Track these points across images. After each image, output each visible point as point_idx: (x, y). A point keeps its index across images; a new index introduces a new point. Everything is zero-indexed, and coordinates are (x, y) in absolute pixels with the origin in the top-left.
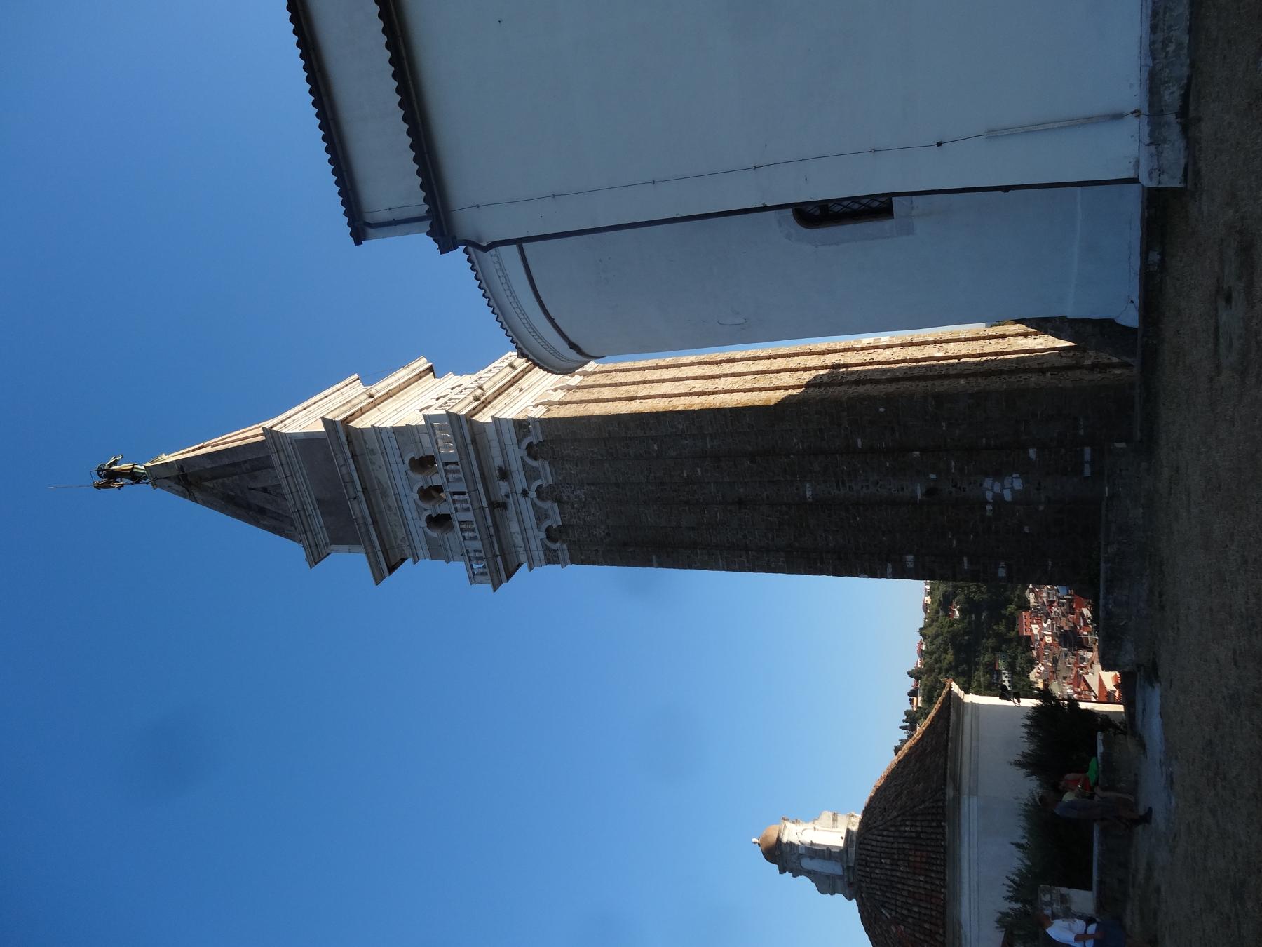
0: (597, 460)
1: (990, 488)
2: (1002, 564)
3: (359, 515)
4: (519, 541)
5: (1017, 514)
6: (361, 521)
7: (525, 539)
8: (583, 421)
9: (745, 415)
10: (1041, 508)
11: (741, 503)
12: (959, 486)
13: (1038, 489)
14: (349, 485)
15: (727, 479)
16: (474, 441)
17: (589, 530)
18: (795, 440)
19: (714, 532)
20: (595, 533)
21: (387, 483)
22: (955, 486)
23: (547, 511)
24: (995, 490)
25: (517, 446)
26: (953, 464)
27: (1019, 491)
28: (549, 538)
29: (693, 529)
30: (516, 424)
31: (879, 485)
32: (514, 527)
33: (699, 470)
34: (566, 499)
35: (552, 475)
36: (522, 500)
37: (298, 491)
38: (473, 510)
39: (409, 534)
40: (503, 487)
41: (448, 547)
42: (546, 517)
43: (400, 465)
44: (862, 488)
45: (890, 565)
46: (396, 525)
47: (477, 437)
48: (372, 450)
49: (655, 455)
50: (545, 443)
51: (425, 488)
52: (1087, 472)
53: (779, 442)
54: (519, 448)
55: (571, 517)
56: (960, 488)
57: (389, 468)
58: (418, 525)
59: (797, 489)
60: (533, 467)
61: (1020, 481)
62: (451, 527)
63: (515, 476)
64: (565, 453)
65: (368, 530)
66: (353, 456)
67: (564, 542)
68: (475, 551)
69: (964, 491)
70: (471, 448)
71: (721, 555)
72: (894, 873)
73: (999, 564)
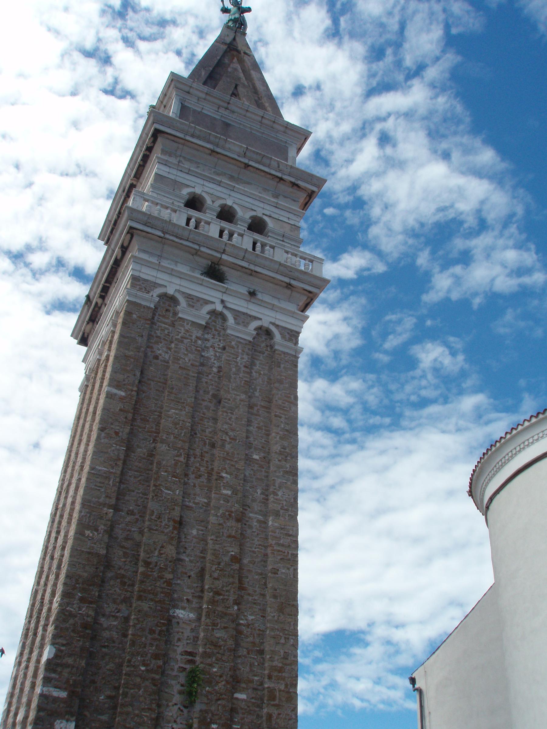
3: (227, 146)
7: (171, 273)
8: (292, 397)
9: (288, 569)
16: (289, 286)
17: (164, 339)
18: (251, 618)
20: (161, 345)
21: (244, 187)
28: (164, 296)
30: (297, 335)
33: (229, 492)
34: (206, 336)
35: (238, 337)
45: (63, 694)
47: (288, 292)
50: (269, 349)
54: (271, 323)
55: (187, 331)
57: (261, 200)
59: (188, 600)
60: (248, 324)
63: (243, 303)
64: (258, 363)
65: (209, 142)
66: (281, 179)
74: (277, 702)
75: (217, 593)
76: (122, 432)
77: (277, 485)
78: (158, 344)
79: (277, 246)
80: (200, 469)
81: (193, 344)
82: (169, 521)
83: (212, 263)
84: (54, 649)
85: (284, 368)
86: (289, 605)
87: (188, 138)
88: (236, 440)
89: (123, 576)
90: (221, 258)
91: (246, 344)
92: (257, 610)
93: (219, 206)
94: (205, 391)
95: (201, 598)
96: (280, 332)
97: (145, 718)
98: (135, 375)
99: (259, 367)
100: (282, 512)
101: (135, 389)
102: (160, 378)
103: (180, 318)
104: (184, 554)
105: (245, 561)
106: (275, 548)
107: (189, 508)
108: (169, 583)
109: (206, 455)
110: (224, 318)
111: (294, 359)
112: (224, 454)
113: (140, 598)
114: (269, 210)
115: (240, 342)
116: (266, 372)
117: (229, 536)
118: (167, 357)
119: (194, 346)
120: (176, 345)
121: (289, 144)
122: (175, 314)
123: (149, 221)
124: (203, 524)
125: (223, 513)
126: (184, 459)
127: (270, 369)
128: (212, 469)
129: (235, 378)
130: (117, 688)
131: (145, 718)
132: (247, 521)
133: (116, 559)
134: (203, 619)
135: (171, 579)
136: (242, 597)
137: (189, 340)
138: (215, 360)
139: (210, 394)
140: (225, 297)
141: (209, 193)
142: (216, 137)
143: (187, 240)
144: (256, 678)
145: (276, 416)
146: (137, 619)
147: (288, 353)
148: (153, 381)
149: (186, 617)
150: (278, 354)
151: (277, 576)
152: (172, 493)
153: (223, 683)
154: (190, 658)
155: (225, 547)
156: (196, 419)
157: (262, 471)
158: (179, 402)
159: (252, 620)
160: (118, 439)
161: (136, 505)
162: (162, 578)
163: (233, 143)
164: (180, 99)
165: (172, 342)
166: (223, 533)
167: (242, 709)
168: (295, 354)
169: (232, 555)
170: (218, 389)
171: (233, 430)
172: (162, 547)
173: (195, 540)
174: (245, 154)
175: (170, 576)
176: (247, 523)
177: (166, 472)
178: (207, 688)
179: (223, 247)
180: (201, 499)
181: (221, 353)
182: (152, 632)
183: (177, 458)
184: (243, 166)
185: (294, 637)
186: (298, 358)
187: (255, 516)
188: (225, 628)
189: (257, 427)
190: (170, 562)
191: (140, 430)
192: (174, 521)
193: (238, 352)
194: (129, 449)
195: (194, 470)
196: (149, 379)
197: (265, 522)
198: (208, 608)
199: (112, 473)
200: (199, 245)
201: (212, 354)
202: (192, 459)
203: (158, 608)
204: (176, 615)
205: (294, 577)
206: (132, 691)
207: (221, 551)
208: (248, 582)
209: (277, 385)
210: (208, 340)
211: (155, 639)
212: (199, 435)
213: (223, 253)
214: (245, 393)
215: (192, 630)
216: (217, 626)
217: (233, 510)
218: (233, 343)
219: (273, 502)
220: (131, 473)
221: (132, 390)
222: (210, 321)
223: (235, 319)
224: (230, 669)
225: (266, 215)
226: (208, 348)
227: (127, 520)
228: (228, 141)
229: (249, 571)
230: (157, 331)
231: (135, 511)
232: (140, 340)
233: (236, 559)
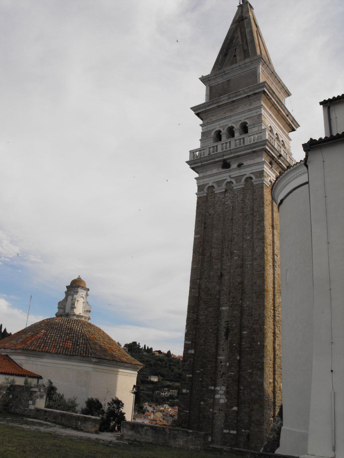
0: (244, 210)
1: (221, 389)
2: (188, 391)
4: (209, 173)
6: (219, 100)
7: (210, 176)
9: (261, 280)
10: (211, 410)
12: (223, 375)
13: (219, 409)
14: (235, 94)
17: (212, 206)
20: (211, 208)
22: (223, 374)
23: (221, 186)
26: (233, 374)
27: (219, 401)
28: (209, 187)
29: (211, 254)
30: (262, 172)
32: (215, 171)
33: (237, 258)
35: (237, 189)
37: (233, 71)
38: (222, 152)
39: (213, 122)
41: (207, 140)
42: (219, 186)
43: (244, 118)
45: (190, 342)
46: (217, 116)
47: (256, 153)
48: (251, 105)
49: (245, 237)
51: (234, 129)
52: (225, 431)
53: (248, 296)
54: (250, 173)
55: (219, 198)
56: (222, 376)
57: (243, 112)
58: (217, 126)
59: (226, 303)
60: (241, 180)
61: (224, 402)
63: (238, 172)
64: (248, 195)
65: (215, 103)
66: (248, 96)
67: (208, 194)
68: (204, 153)
69: (221, 377)
70: (250, 151)
72: (64, 334)
73: (188, 390)
74: (256, 332)
75: (234, 298)
77: (255, 247)
83: (223, 162)
85: (257, 192)
87: (207, 108)
91: (241, 190)
94: (228, 219)
97: (213, 346)
98: (202, 227)
99: (249, 196)
100: (258, 257)
103: (216, 193)
105: (246, 282)
107: (224, 269)
114: (248, 115)
115: (239, 191)
116: (252, 197)
118: (213, 212)
121: (256, 67)
123: (195, 162)
129: (237, 208)
131: (213, 346)
132: (246, 266)
140: (231, 173)
142: (216, 100)
143: (210, 160)
145: (255, 216)
147: (259, 184)
149: (226, 309)
151: (256, 284)
153: (237, 329)
154: (227, 323)
158: (217, 230)
167: (245, 337)
169: (239, 282)
172: (215, 287)
173: (227, 281)
176: (246, 267)
178: (232, 332)
183: (218, 252)
187: (248, 263)
193: (238, 196)
202: (225, 249)
203: (215, 309)
212: (227, 239)
217: (239, 264)
223: (236, 181)
224: (239, 324)
225: (246, 119)
226: (228, 200)
227: (205, 281)
231: (207, 277)
233: (242, 283)
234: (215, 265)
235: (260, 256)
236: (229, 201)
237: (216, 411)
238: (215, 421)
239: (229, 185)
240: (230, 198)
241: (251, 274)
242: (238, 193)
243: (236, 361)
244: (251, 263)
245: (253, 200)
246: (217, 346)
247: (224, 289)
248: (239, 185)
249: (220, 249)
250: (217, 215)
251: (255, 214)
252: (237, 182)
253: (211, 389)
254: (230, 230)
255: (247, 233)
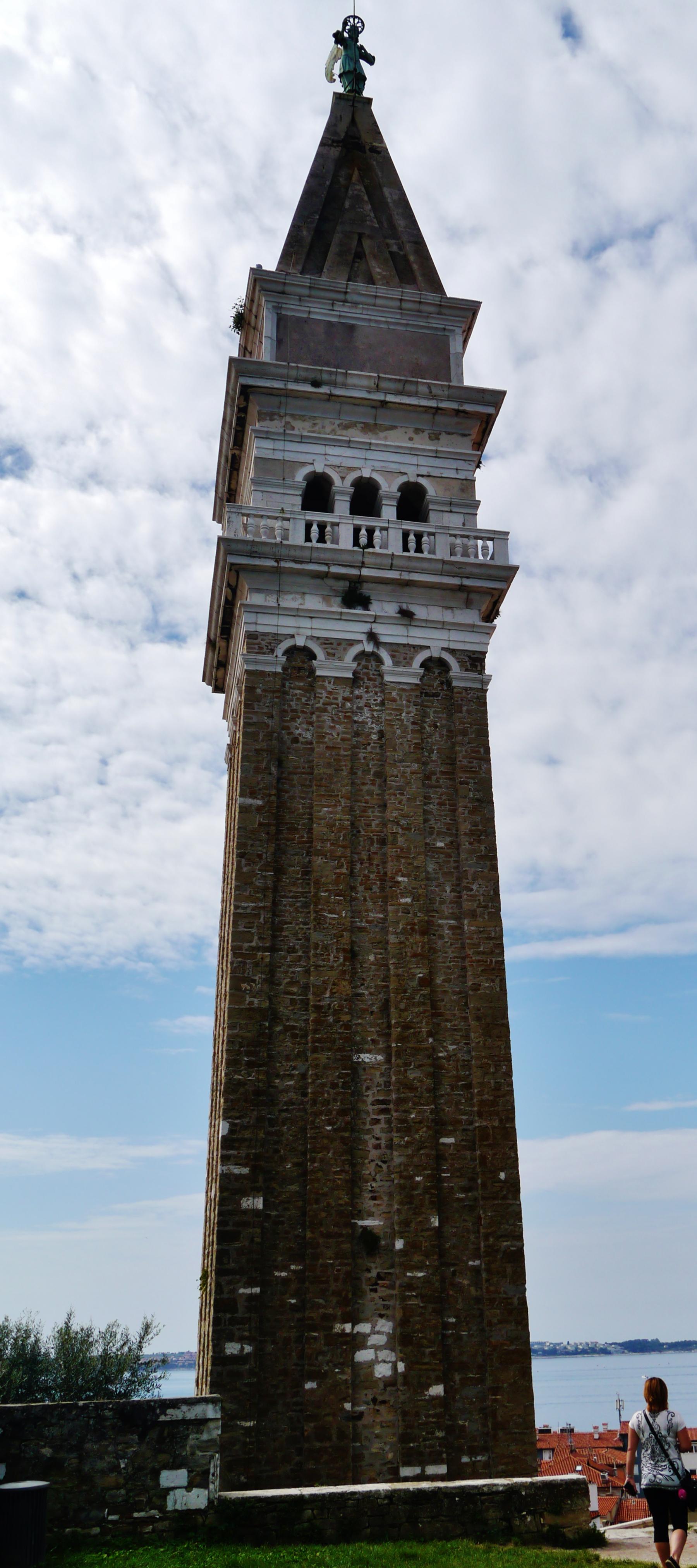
1: (377, 1329)
4: (289, 602)
5: (337, 1370)
7: (296, 613)
8: (482, 750)
9: (493, 981)
10: (348, 1406)
11: (352, 955)
12: (379, 1282)
13: (374, 1400)
14: (399, 386)
15: (392, 939)
17: (303, 712)
18: (451, 1048)
19: (299, 904)
20: (299, 721)
21: (386, 438)
22: (379, 1277)
23: (341, 659)
24: (376, 1336)
25: (446, 646)
27: (372, 1374)
28: (291, 652)
30: (482, 656)
31: (380, 1163)
32: (313, 603)
33: (409, 900)
34: (357, 692)
35: (399, 683)
36: (365, 628)
40: (390, 609)
44: (378, 1139)
50: (445, 688)
53: (449, 1025)
54: (443, 649)
55: (330, 693)
56: (377, 1284)
60: (412, 659)
62: (306, 506)
64: (431, 712)
67: (284, 669)
69: (371, 1290)
70: (456, 581)
71: (264, 908)
76: (266, 853)
77: (470, 877)
78: (296, 721)
79: (438, 531)
80: (369, 877)
81: (340, 709)
82: (337, 952)
84: (228, 1124)
85: (469, 712)
86: (498, 1025)
88: (411, 829)
89: (294, 1028)
90: (360, 575)
92: (459, 1037)
93: (352, 485)
95: (389, 1035)
96: (457, 659)
97: (339, 1182)
98: (270, 774)
100: (479, 910)
101: (274, 792)
102: (304, 768)
104: (362, 987)
105: (439, 981)
106: (474, 958)
107: (361, 929)
108: (347, 1026)
109: (375, 856)
110: (380, 661)
111: (480, 694)
112: (397, 851)
113: (315, 1050)
115: (403, 690)
116: (444, 722)
117: (415, 955)
118: (308, 735)
119: (342, 712)
120: (318, 717)
122: (312, 671)
123: (255, 549)
124: (381, 945)
125: (403, 929)
126: (347, 869)
127: (450, 715)
128: (385, 873)
130: (304, 1154)
132: (436, 931)
133: (281, 1009)
134: (393, 1060)
135: (350, 1021)
136: (439, 1025)
137: (334, 706)
138: (372, 723)
139: (372, 773)
141: (335, 466)
142: (331, 373)
144: (464, 1117)
145: (461, 783)
146: (316, 1075)
147: (471, 689)
148: (296, 774)
150: (457, 693)
151: (479, 992)
152: (337, 916)
153: (425, 1129)
154: (383, 1106)
155: (410, 969)
156: (358, 812)
157: (449, 862)
158: (331, 796)
159: (454, 1050)
160: (262, 863)
161: (297, 940)
162: (339, 1021)
163: (357, 375)
164: (274, 307)
165: (312, 713)
166: (406, 952)
168: (480, 687)
169: (419, 978)
170: (380, 763)
171: (405, 816)
173: (373, 967)
174: (377, 386)
175: (348, 1017)
176: (437, 933)
177: (326, 891)
179: (360, 558)
180: (375, 915)
181: (381, 710)
182: (334, 1086)
183: (338, 871)
184: (379, 404)
185: (506, 1063)
186: (487, 690)
188: (420, 1066)
189: (438, 804)
190: (345, 1001)
191: (288, 843)
192: (344, 950)
193: (402, 705)
194: (279, 871)
195: (362, 880)
196: (290, 773)
197: (460, 927)
198: (397, 1046)
199: (261, 907)
200: (326, 564)
201: (368, 715)
202: (358, 866)
203: (339, 1057)
204: (360, 1060)
205: (501, 990)
206: (320, 1155)
207: (406, 975)
208: (445, 1006)
209: (459, 738)
210: (359, 697)
211: (338, 1093)
212: (363, 833)
213: (362, 567)
214: (417, 761)
215: (382, 1075)
216: (411, 1065)
218: (394, 694)
219: (467, 900)
220: (285, 901)
221: (270, 795)
222: (360, 667)
223: (393, 656)
225: (422, 476)
228: (350, 374)
229: (445, 992)
230: (291, 703)
232: (270, 722)
233: (427, 982)
234: (330, 913)
235: (486, 907)
236: (367, 713)
237: (363, 1408)
238: (360, 1442)
239: (363, 663)
240: (367, 705)
241: (455, 957)
242: (401, 698)
243: (426, 1234)
244: (452, 922)
245: (451, 734)
246: (354, 1183)
247: (363, 994)
248: (401, 674)
249: (343, 859)
250: (327, 748)
251: (462, 776)
252: (396, 663)
253: (344, 1330)
254: (374, 807)
255: (434, 828)
